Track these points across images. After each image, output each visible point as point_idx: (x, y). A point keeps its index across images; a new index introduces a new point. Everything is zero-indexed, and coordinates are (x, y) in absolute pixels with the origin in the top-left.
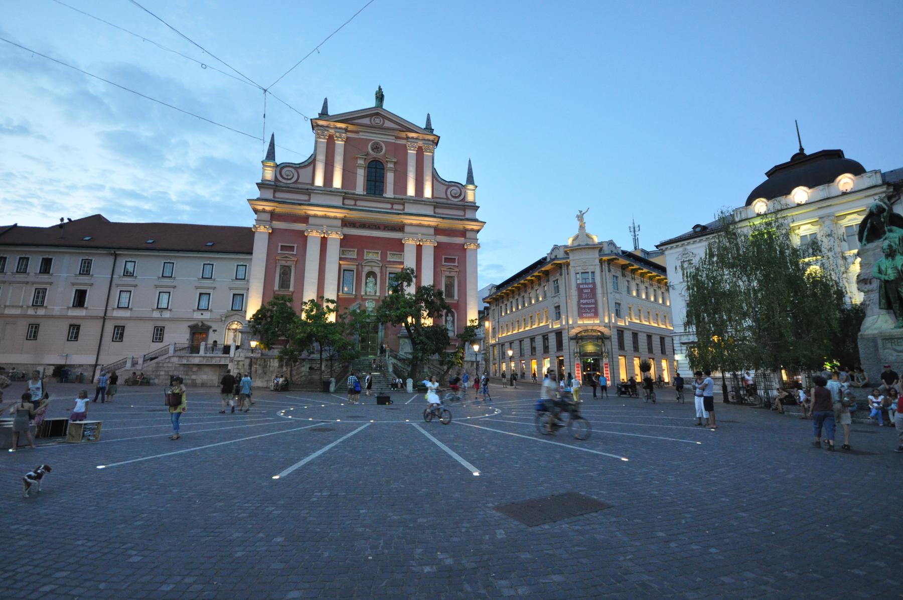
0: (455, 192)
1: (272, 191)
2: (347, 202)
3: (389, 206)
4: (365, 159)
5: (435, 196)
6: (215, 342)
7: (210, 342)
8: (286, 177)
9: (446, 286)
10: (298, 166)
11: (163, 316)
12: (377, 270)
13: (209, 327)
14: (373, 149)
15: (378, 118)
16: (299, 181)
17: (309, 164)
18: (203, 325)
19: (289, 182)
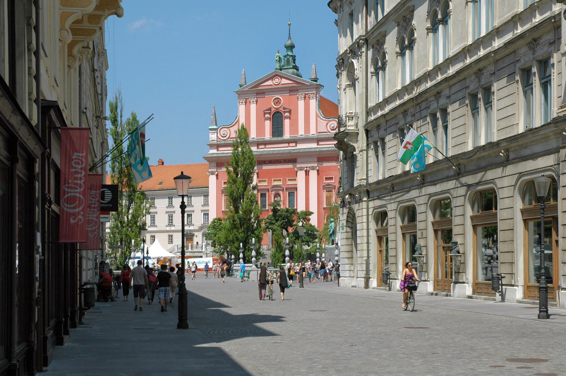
0: (332, 125)
1: (216, 147)
2: (260, 147)
3: (287, 145)
4: (270, 112)
5: (318, 131)
6: (197, 243)
7: (195, 243)
8: (223, 136)
9: (327, 198)
10: (229, 126)
11: (171, 229)
12: (281, 192)
13: (193, 235)
14: (274, 104)
15: (277, 78)
16: (230, 137)
17: (236, 123)
18: (190, 233)
19: (225, 138)
